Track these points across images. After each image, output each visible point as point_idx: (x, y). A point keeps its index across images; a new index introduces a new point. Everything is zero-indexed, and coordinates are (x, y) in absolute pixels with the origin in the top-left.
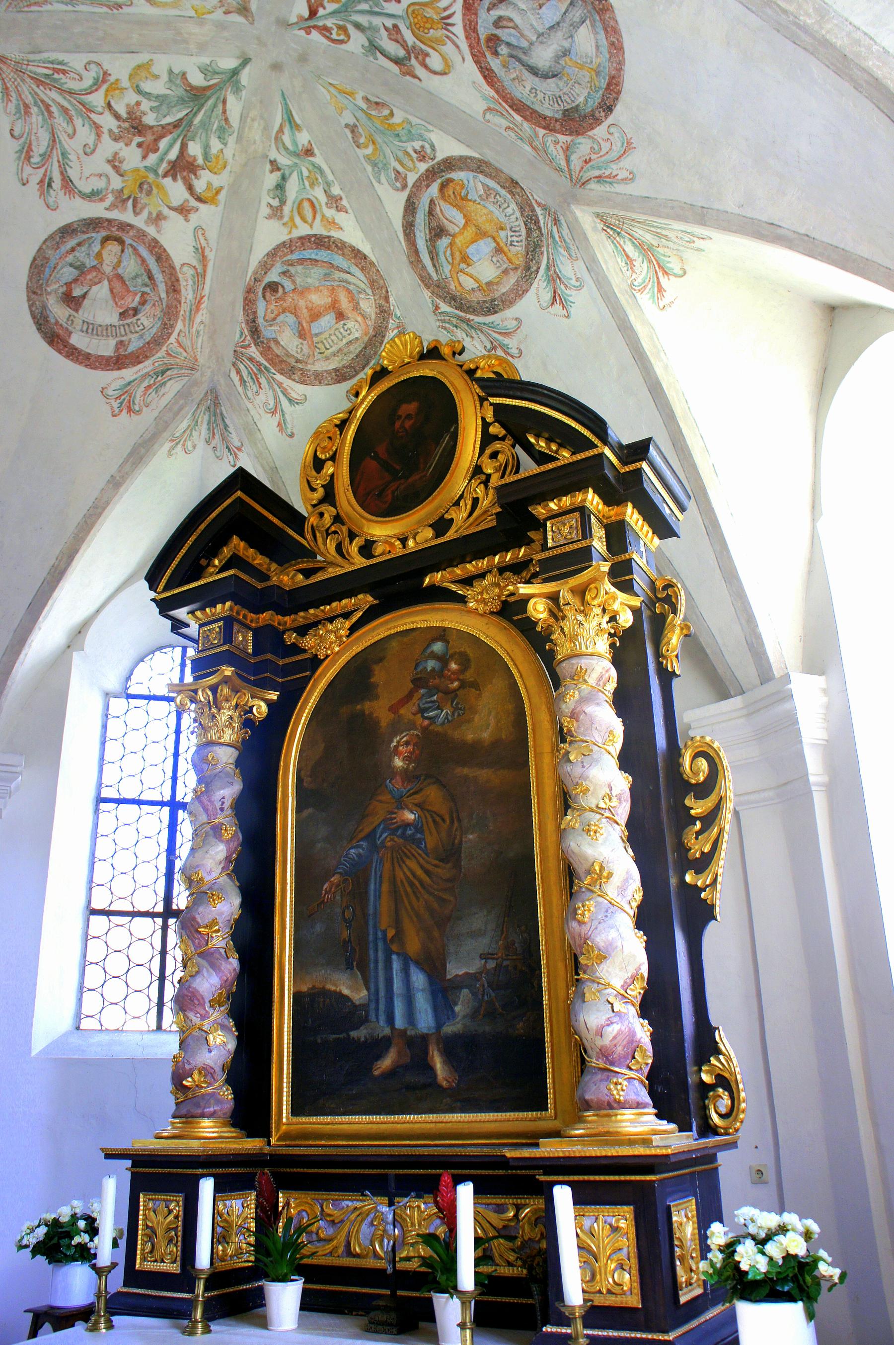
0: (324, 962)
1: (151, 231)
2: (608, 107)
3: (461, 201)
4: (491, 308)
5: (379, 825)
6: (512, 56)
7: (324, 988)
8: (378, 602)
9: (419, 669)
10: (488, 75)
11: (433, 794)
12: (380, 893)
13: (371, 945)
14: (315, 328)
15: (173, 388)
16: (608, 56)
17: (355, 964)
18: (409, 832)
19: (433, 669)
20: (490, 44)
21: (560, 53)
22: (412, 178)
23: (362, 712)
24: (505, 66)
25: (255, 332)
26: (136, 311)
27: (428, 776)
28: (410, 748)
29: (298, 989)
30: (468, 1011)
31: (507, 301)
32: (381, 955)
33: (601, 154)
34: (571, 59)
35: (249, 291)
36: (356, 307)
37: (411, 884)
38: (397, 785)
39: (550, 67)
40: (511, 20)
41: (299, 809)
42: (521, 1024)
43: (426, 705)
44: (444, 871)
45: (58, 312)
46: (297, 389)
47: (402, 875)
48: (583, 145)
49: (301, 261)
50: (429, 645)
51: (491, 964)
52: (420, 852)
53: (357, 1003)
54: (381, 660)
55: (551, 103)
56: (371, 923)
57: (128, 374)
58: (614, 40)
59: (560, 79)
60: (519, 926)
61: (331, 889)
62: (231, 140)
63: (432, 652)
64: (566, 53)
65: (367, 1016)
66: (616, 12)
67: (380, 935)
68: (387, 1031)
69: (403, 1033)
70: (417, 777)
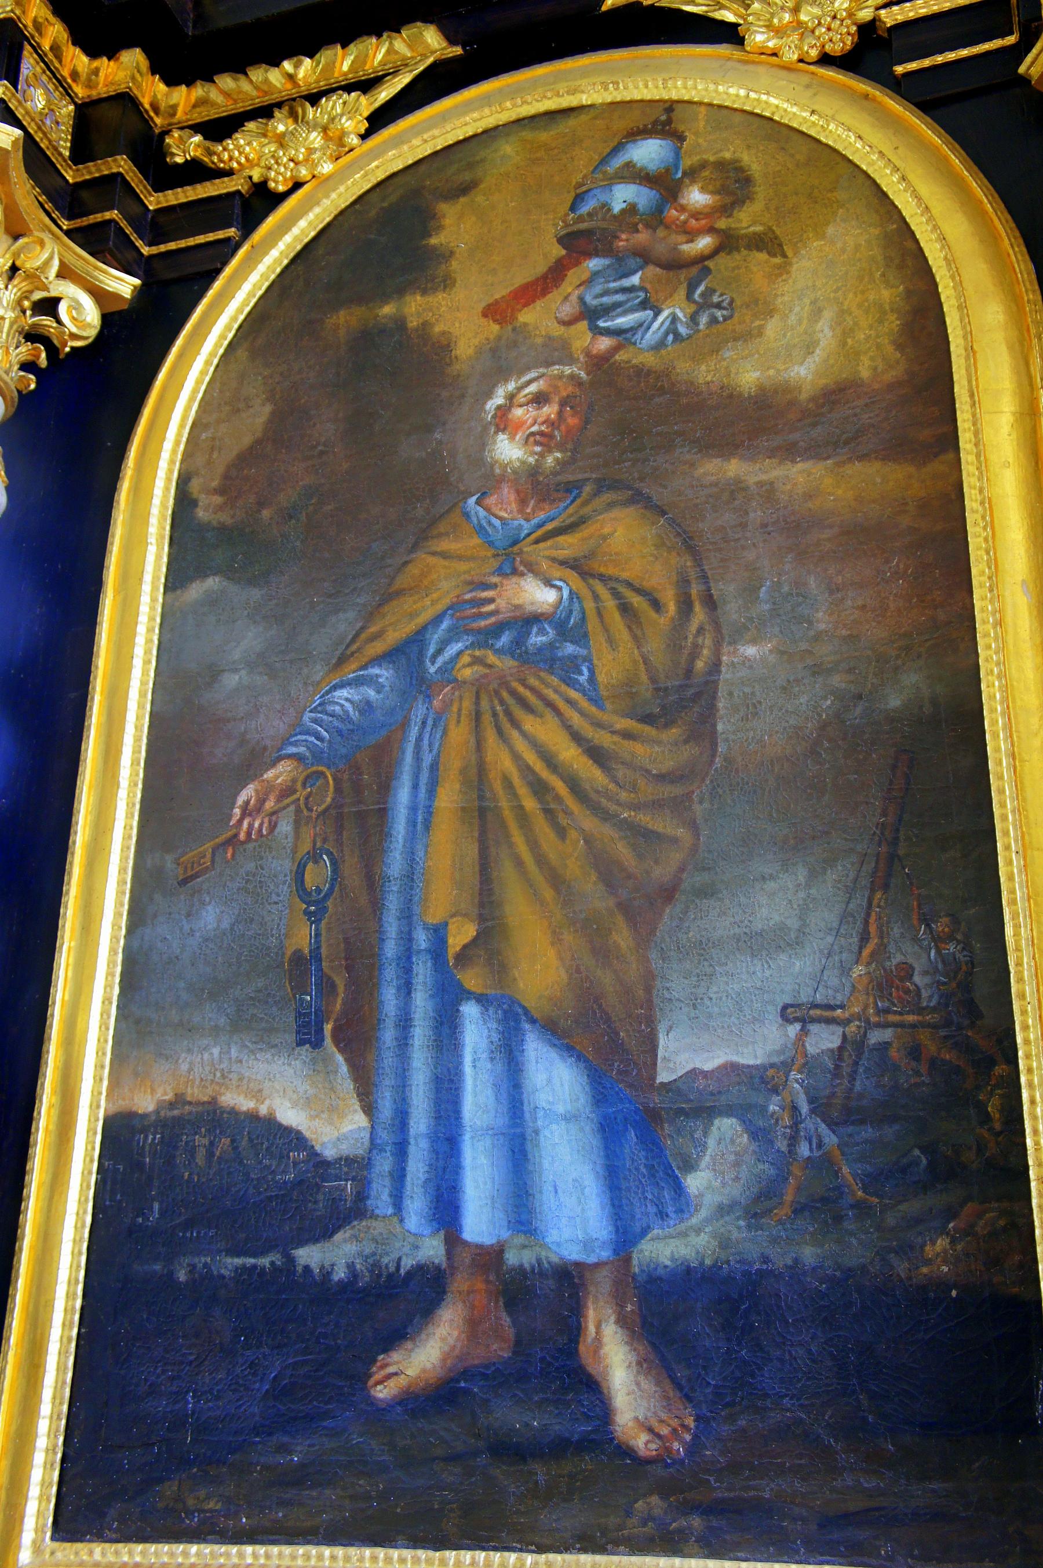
0: (222, 1021)
5: (438, 619)
7: (213, 1102)
8: (458, 50)
9: (585, 209)
11: (624, 536)
12: (429, 812)
13: (390, 973)
17: (328, 1028)
18: (536, 639)
19: (631, 209)
23: (400, 323)
27: (602, 485)
28: (550, 411)
29: (122, 1105)
30: (735, 1191)
32: (422, 1002)
37: (539, 789)
38: (504, 510)
41: (176, 578)
42: (942, 1243)
43: (605, 300)
44: (659, 750)
47: (507, 764)
50: (616, 150)
51: (824, 1040)
52: (574, 694)
53: (329, 1153)
54: (465, 189)
56: (393, 904)
60: (927, 921)
61: (261, 801)
63: (629, 165)
65: (361, 1196)
67: (422, 939)
68: (432, 1249)
69: (490, 1258)
70: (571, 488)
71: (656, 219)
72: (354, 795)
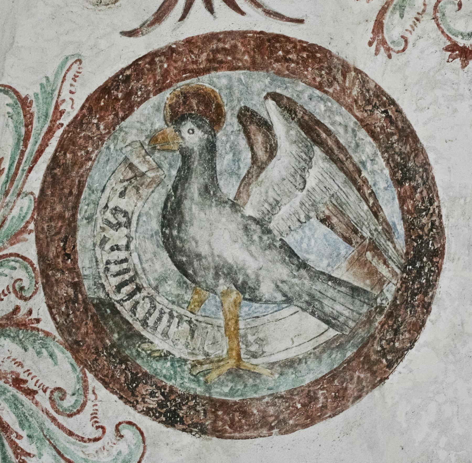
2: (175, 413)
6: (186, 156)
10: (115, 98)
16: (282, 390)
20: (194, 102)
21: (241, 278)
24: (155, 142)
33: (60, 419)
34: (237, 304)
39: (199, 256)
40: (272, 151)
48: (56, 369)
55: (114, 268)
58: (321, 399)
59: (180, 284)
64: (247, 290)
66: (376, 392)
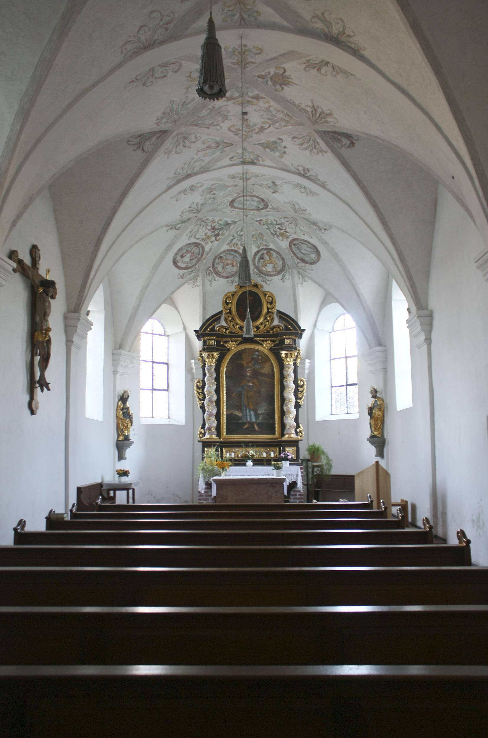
1: (204, 245)
3: (270, 256)
4: (267, 275)
11: (255, 381)
14: (227, 267)
15: (193, 274)
22: (261, 248)
25: (213, 265)
26: (193, 259)
31: (271, 276)
35: (216, 257)
36: (237, 265)
38: (248, 378)
41: (226, 379)
45: (179, 258)
46: (217, 278)
48: (303, 264)
49: (229, 254)
57: (185, 271)
62: (228, 231)
71: (257, 358)
72: (240, 395)
